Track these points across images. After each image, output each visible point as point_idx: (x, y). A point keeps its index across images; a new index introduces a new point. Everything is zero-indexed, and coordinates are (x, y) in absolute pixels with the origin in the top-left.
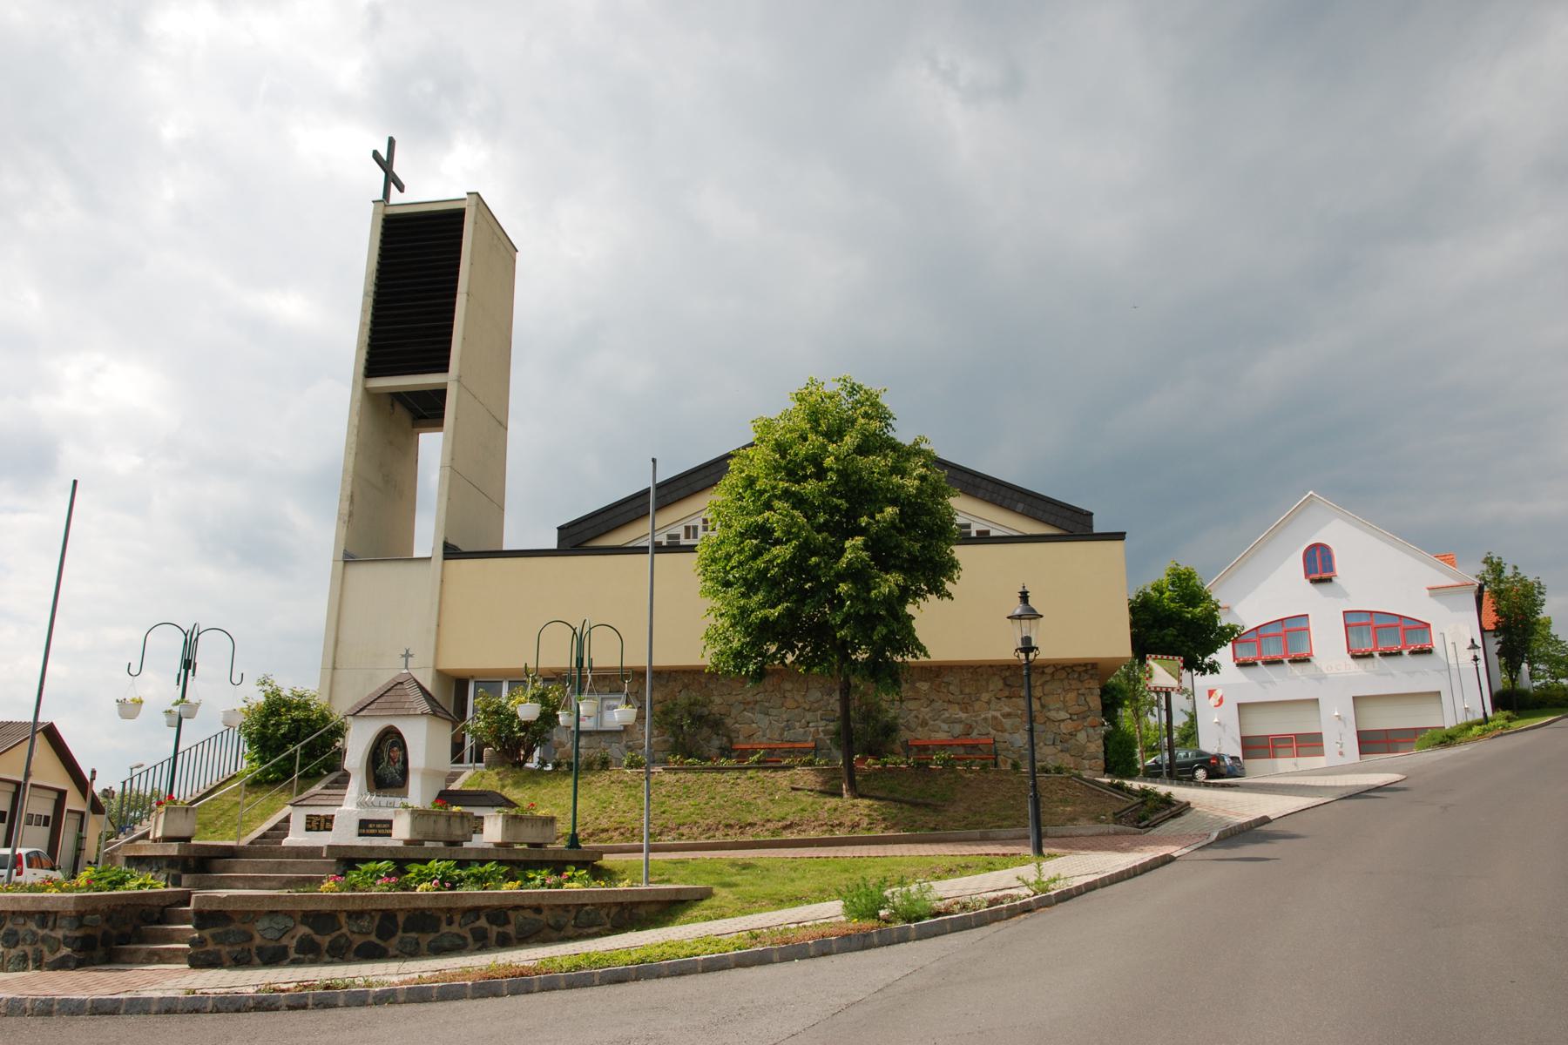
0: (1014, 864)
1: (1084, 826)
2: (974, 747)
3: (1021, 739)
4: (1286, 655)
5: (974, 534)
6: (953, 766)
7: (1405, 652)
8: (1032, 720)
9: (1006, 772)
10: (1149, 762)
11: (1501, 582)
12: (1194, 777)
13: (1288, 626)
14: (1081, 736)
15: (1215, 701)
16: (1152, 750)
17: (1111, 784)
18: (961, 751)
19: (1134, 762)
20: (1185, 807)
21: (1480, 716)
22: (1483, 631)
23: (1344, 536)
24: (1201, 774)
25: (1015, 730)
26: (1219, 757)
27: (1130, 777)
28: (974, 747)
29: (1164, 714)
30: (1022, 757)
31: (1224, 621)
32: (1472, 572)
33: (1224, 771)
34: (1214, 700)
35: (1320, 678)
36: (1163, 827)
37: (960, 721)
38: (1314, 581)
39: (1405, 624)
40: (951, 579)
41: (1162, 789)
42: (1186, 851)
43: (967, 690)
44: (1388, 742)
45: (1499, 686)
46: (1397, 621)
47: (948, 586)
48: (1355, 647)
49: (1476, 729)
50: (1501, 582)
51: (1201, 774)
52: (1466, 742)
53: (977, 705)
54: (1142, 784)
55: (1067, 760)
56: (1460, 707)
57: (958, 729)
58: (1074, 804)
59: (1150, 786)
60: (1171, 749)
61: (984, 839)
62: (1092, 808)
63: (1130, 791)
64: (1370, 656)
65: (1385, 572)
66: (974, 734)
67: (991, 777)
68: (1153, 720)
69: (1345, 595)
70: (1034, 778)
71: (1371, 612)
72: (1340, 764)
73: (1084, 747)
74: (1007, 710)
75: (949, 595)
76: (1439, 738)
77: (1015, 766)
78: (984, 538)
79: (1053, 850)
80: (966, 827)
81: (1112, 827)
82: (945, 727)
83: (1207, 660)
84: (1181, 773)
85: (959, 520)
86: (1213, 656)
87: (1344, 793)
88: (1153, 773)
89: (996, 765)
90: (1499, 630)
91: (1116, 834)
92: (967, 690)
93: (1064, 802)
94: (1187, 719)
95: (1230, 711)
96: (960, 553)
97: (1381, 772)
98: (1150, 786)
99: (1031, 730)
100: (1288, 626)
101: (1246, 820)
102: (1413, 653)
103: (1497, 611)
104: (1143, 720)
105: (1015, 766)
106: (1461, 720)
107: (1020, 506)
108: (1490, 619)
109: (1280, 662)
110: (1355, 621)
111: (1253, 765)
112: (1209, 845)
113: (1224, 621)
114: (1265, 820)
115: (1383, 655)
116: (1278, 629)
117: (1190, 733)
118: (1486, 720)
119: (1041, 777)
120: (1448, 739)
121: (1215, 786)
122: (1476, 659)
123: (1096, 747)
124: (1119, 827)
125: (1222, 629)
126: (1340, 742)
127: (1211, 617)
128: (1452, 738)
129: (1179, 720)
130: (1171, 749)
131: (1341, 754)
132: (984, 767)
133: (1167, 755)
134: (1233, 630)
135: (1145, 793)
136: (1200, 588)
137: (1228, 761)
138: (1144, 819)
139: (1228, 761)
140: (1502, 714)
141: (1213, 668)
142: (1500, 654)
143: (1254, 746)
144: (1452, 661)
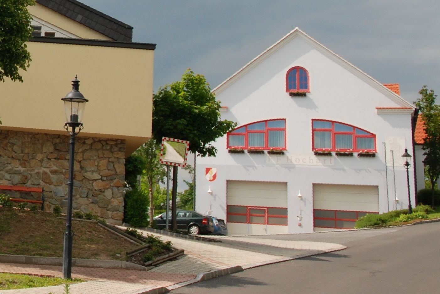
0: (49, 284)
1: (104, 261)
2: (28, 193)
3: (63, 191)
4: (267, 148)
5: (43, 35)
6: (11, 206)
7: (355, 154)
8: (72, 178)
9: (50, 215)
10: (157, 217)
11: (432, 108)
12: (189, 232)
13: (270, 126)
14: (108, 194)
15: (211, 177)
16: (159, 209)
17: (127, 231)
18: (18, 195)
19: (145, 217)
20: (181, 253)
21: (406, 207)
22: (414, 144)
23: (316, 62)
24: (194, 230)
25: (59, 184)
26: (209, 219)
27: (142, 227)
28: (28, 193)
29: (171, 182)
30: (62, 204)
31: (222, 117)
32: (411, 99)
33: (212, 229)
34: (209, 176)
35: (290, 167)
36: (162, 267)
37: (19, 173)
38: (293, 95)
39: (358, 133)
40: (22, 66)
41: (164, 238)
42: (177, 286)
43: (26, 151)
44: (336, 219)
45: (422, 186)
46: (352, 130)
47: (20, 71)
48: (318, 147)
49: (402, 217)
50: (432, 108)
51: (194, 230)
52: (394, 226)
53: (33, 163)
54: (150, 233)
55: (95, 210)
56: (392, 198)
57: (17, 179)
58: (98, 243)
59: (155, 235)
60: (174, 209)
61: (28, 263)
62: (111, 247)
63: (140, 237)
64: (329, 154)
65: (345, 93)
66: (29, 184)
67: (38, 216)
68: (162, 187)
69: (313, 106)
70: (70, 221)
71: (333, 122)
72: (298, 232)
73: (109, 202)
74: (54, 168)
75: (20, 79)
76: (374, 221)
77: (57, 210)
78: (50, 38)
79: (79, 276)
80: (15, 252)
81: (124, 263)
82: (7, 176)
83: (207, 146)
84: (180, 228)
85: (33, 23)
86: (212, 143)
87: (300, 254)
88: (159, 226)
89: (42, 208)
90: (427, 144)
91: (127, 268)
92: (26, 151)
93: (91, 241)
94: (187, 188)
95: (220, 187)
96: (31, 47)
97: (328, 242)
98: (155, 235)
99: (71, 185)
100: (270, 126)
101: (224, 267)
102: (361, 155)
103: (427, 131)
104: (155, 186)
105: (57, 210)
106: (392, 209)
107: (80, 17)
108: (421, 136)
109: (261, 152)
110: (320, 127)
111: (233, 227)
112: (195, 284)
113: (222, 117)
114: (238, 269)
115: (339, 154)
116: (263, 128)
117: (190, 199)
118: (410, 210)
119: (76, 221)
120: (381, 222)
121: (204, 240)
122: (407, 164)
123: (118, 202)
124: (129, 264)
125: (221, 123)
126: (300, 216)
127: (213, 114)
128: (384, 221)
129: (182, 188)
130: (174, 209)
131: (300, 225)
132: (33, 209)
133: (170, 214)
134: (229, 125)
135: (151, 240)
136: (207, 91)
137: (215, 223)
138: (149, 259)
139: (215, 223)
140: (423, 207)
141: (212, 152)
142: (425, 162)
143: (235, 213)
144: (389, 164)
